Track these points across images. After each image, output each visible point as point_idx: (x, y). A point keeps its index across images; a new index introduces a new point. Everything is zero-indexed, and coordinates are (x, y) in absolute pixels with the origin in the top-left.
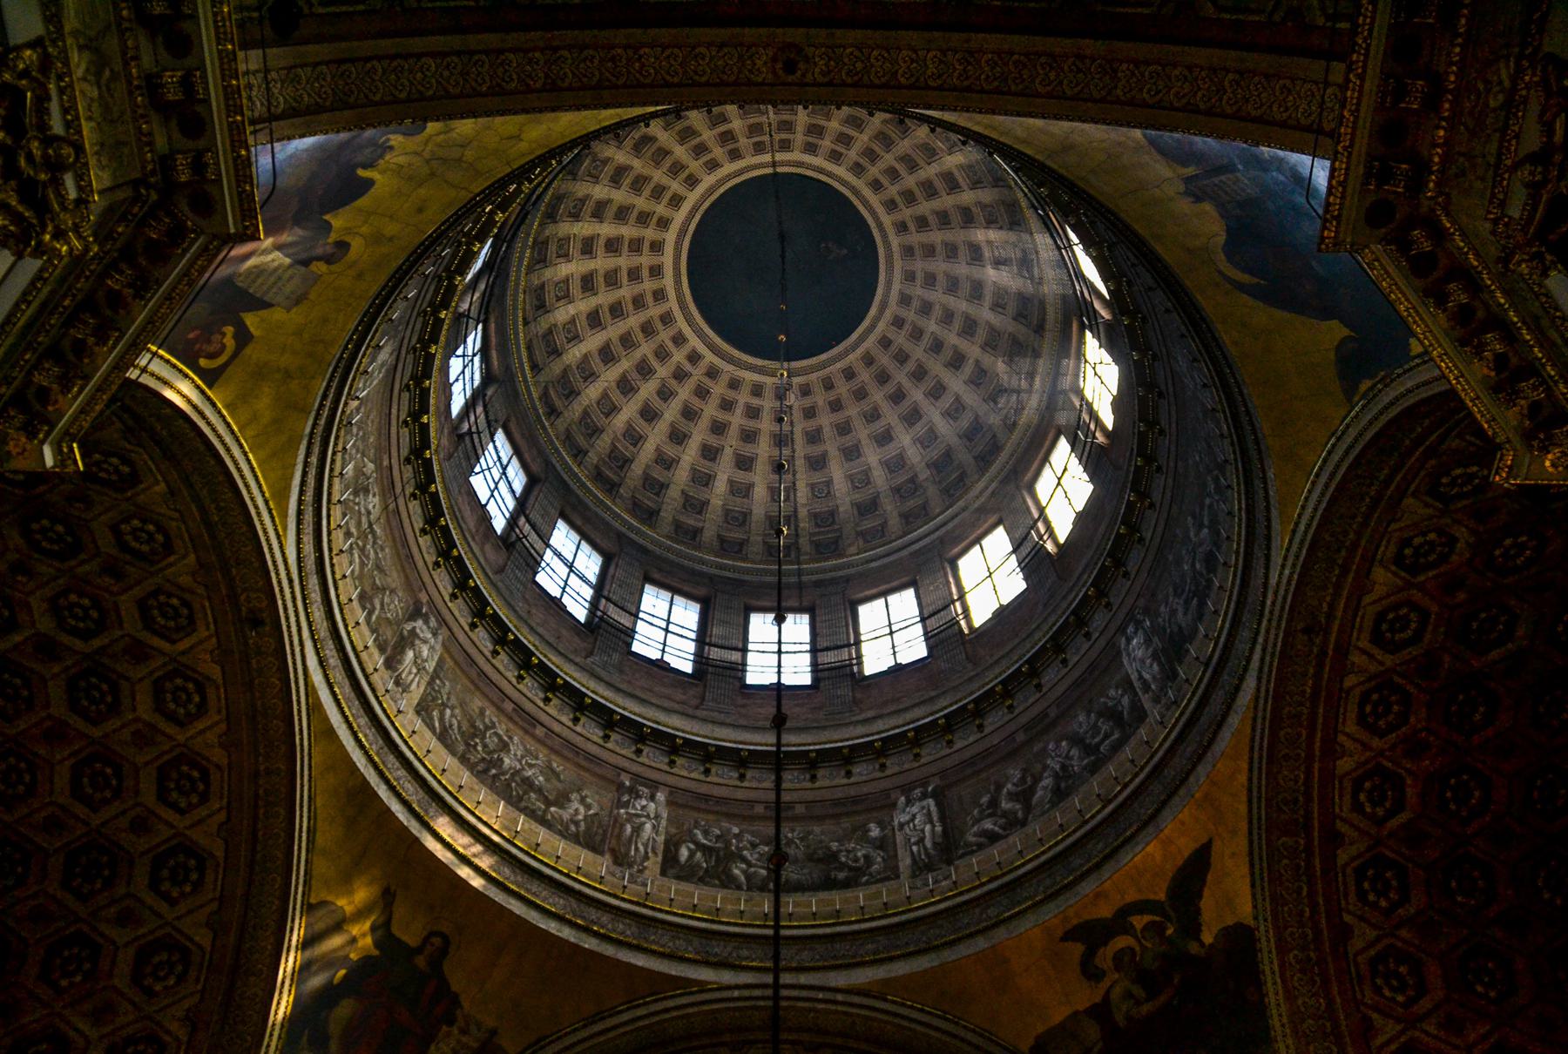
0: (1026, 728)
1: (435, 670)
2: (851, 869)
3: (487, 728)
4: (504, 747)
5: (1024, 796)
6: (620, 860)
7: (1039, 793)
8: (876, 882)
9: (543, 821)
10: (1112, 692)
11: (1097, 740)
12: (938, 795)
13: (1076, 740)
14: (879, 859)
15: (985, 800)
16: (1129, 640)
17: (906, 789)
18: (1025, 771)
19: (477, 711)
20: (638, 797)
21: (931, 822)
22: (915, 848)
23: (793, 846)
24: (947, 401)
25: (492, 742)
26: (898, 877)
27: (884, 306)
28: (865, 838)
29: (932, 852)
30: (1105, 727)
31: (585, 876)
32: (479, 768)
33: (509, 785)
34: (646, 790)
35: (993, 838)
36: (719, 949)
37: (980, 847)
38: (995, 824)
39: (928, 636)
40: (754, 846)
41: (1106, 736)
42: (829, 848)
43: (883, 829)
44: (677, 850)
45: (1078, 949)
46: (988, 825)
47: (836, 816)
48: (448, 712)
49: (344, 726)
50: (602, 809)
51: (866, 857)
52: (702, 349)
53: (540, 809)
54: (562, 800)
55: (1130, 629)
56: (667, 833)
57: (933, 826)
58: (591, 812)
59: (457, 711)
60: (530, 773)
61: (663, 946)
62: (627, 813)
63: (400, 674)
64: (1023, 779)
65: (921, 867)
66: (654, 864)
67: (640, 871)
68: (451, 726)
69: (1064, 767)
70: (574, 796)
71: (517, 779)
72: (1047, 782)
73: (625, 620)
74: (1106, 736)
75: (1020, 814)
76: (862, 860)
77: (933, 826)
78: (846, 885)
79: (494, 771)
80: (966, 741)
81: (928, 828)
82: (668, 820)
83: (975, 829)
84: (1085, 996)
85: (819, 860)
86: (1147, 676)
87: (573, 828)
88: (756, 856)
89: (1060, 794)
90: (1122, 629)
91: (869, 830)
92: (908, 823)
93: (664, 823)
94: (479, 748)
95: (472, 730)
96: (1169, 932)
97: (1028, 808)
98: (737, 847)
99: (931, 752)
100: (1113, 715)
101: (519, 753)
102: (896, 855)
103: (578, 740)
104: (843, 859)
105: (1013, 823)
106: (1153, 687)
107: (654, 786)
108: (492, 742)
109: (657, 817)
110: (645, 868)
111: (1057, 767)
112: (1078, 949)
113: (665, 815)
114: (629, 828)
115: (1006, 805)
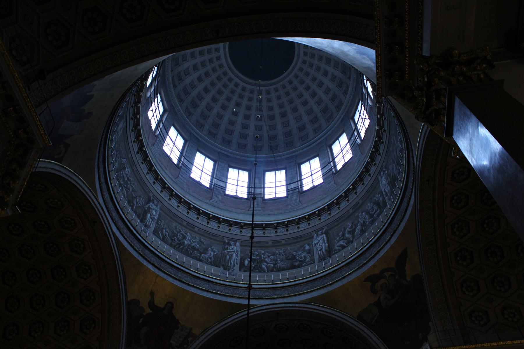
0: (353, 208)
1: (158, 218)
2: (300, 261)
3: (178, 232)
4: (184, 237)
5: (352, 232)
6: (226, 268)
7: (357, 231)
8: (307, 265)
9: (200, 260)
10: (377, 196)
11: (373, 212)
12: (326, 233)
13: (368, 213)
14: (309, 257)
15: (341, 234)
16: (381, 177)
17: (316, 231)
18: (353, 223)
19: (174, 227)
20: (231, 245)
21: (324, 243)
22: (319, 252)
23: (282, 255)
25: (180, 237)
26: (314, 263)
27: (299, 57)
28: (304, 250)
29: (325, 253)
30: (376, 208)
31: (215, 276)
32: (177, 247)
33: (187, 250)
34: (233, 243)
35: (343, 247)
37: (340, 250)
38: (344, 243)
40: (269, 256)
41: (376, 211)
42: (293, 255)
43: (309, 246)
44: (244, 262)
46: (342, 243)
47: (295, 243)
48: (164, 230)
49: (129, 246)
50: (219, 252)
51: (304, 256)
52: (239, 81)
53: (198, 256)
54: (205, 251)
55: (382, 173)
56: (240, 256)
57: (325, 244)
58: (215, 253)
59: (167, 230)
60: (194, 244)
61: (241, 295)
62: (227, 252)
63: (146, 223)
64: (352, 226)
65: (322, 259)
66: (237, 267)
67: (232, 271)
68: (166, 235)
69: (364, 222)
70: (209, 249)
71: (190, 247)
72: (359, 227)
73: (222, 184)
74: (376, 211)
75: (351, 239)
76: (303, 258)
77: (325, 244)
78: (298, 267)
79: (182, 247)
80: (335, 212)
81: (323, 244)
82: (241, 252)
83: (338, 244)
85: (290, 259)
86: (387, 191)
87: (210, 260)
88: (269, 260)
89: (363, 232)
90: (379, 173)
91: (305, 247)
92: (317, 243)
93: (239, 253)
94: (176, 240)
95: (173, 234)
96: (397, 277)
97: (353, 237)
98: (263, 258)
99: (324, 217)
100: (378, 204)
101: (190, 238)
102: (314, 255)
103: (209, 230)
104: (297, 258)
105: (350, 242)
106: (388, 195)
107: (235, 241)
108: (180, 237)
109: (237, 251)
110: (234, 269)
111: (362, 222)
113: (239, 250)
114: (228, 257)
115: (347, 235)
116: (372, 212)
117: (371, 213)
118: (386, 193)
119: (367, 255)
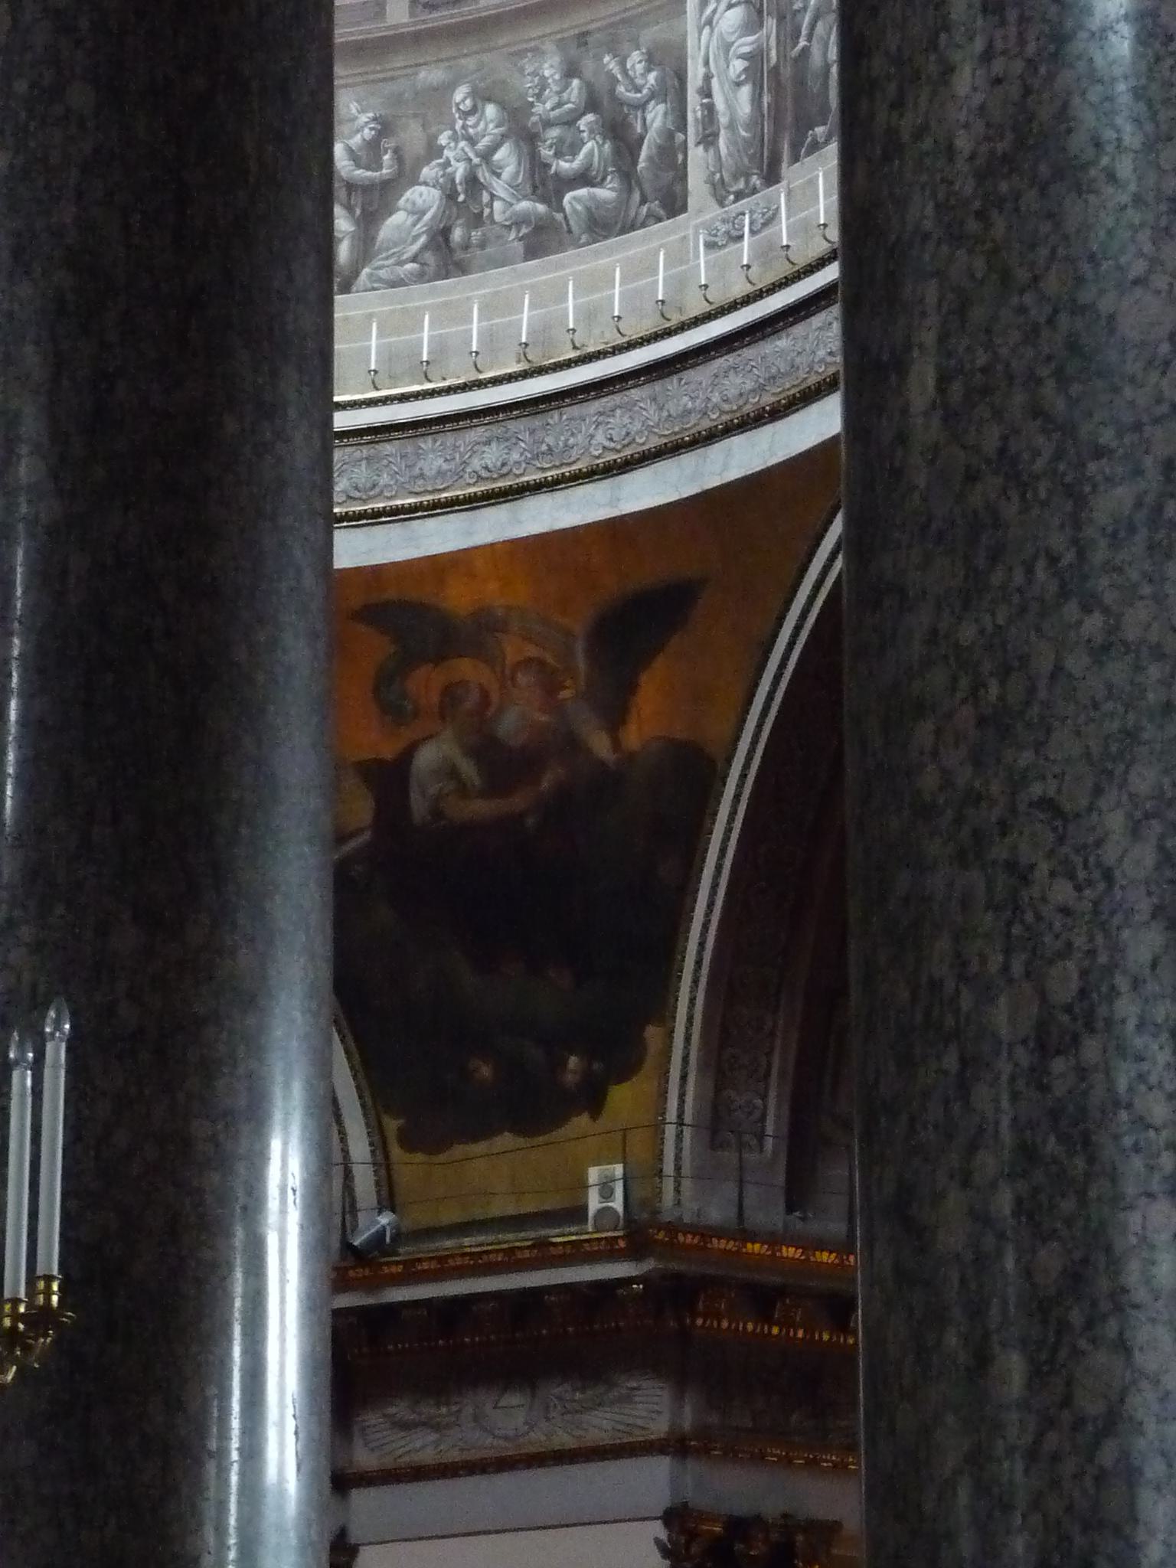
10: (636, 61)
11: (565, 166)
18: (385, 128)
30: (593, 149)
41: (584, 178)
64: (374, 147)
69: (473, 182)
74: (584, 178)
111: (460, 171)
116: (558, 155)
117: (546, 153)
118: (710, 110)
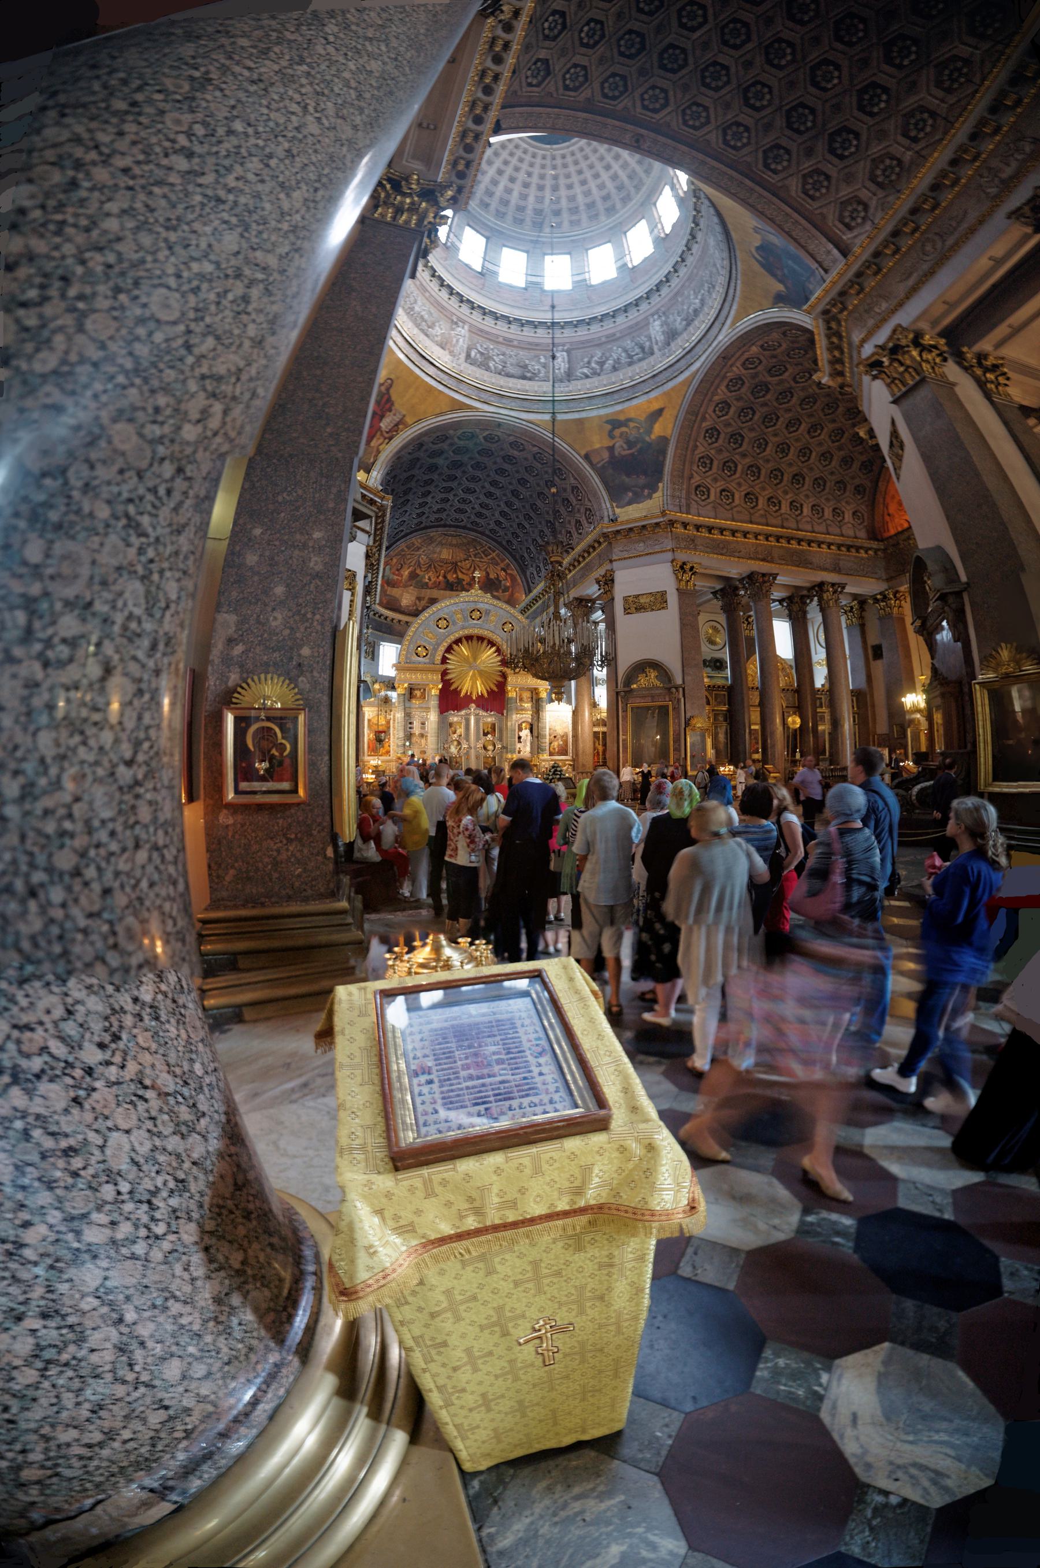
13: (626, 351)
24: (599, 181)
30: (637, 350)
35: (587, 377)
36: (484, 396)
39: (574, 282)
45: (609, 427)
46: (585, 370)
72: (611, 362)
78: (530, 379)
84: (607, 443)
89: (615, 369)
90: (653, 315)
97: (602, 370)
100: (642, 348)
105: (595, 373)
112: (609, 427)
115: (593, 365)
119: (616, 396)
